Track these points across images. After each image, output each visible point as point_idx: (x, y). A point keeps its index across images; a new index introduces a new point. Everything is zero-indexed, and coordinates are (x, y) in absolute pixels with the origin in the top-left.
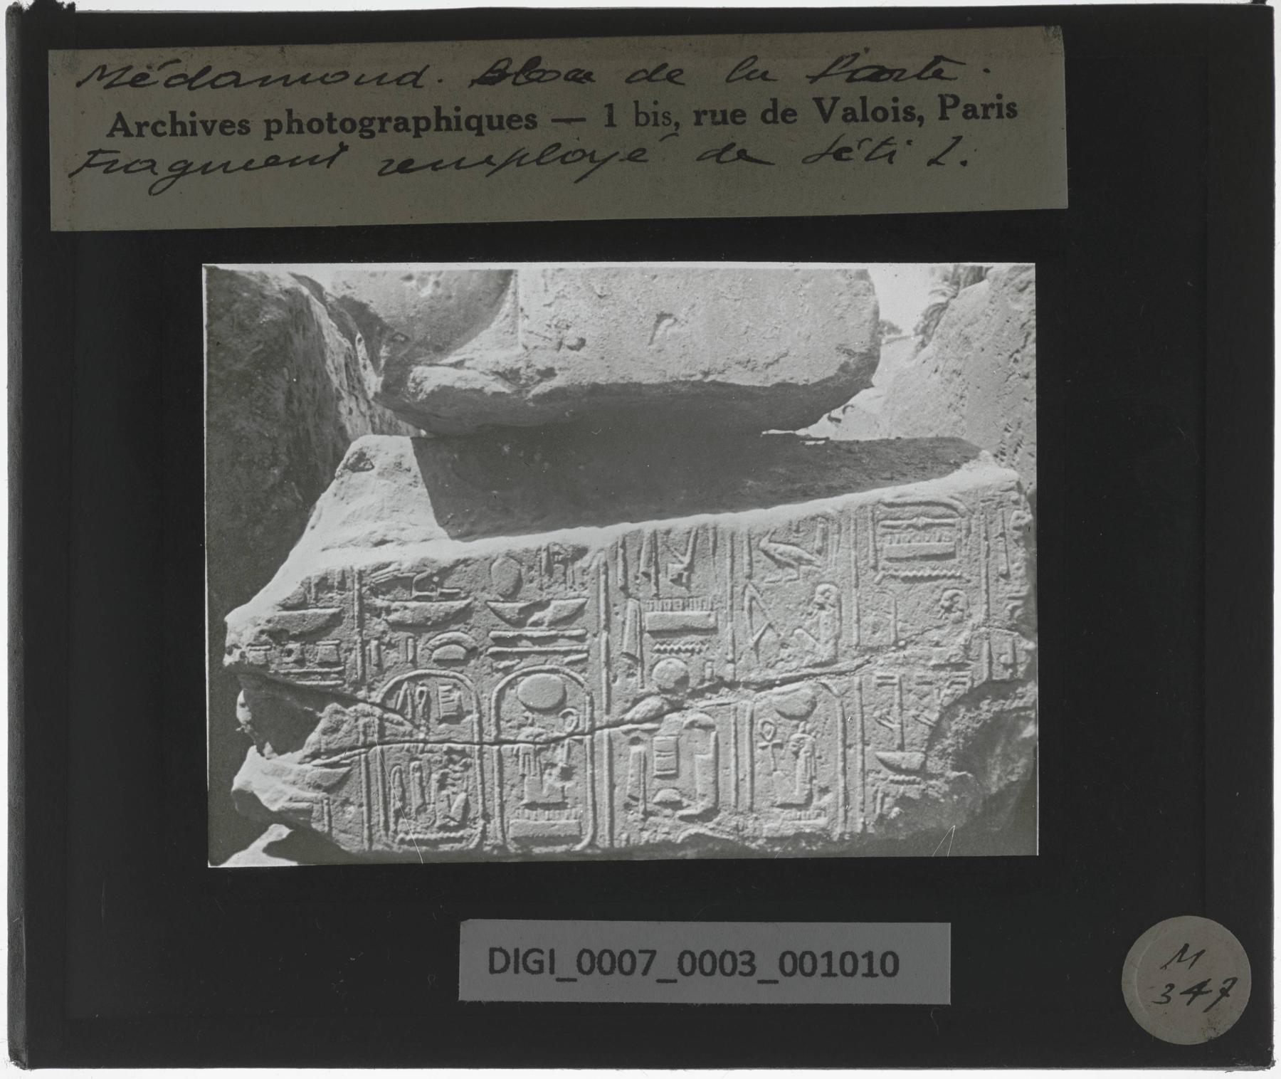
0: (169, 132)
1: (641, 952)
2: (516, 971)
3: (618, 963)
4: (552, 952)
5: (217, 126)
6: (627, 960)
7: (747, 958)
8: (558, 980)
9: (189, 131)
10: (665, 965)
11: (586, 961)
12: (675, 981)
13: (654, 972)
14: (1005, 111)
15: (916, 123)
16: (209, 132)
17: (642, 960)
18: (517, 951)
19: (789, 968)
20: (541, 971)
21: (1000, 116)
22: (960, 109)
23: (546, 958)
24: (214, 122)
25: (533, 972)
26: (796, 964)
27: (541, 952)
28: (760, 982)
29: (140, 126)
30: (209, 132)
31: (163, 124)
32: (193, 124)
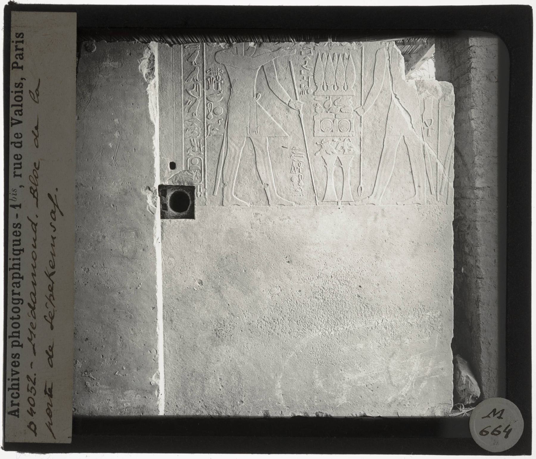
0: (17, 391)
5: (14, 369)
9: (16, 382)
14: (21, 39)
15: (23, 81)
16: (17, 373)
21: (22, 42)
22: (18, 61)
24: (12, 370)
29: (13, 405)
30: (17, 373)
31: (13, 394)
32: (12, 380)
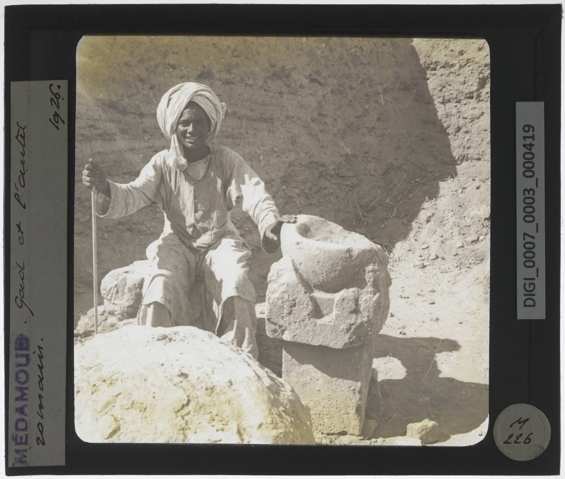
1: (524, 240)
2: (534, 295)
3: (530, 249)
4: (525, 279)
6: (528, 246)
7: (526, 192)
8: (537, 276)
10: (530, 228)
11: (528, 264)
12: (537, 224)
13: (532, 232)
17: (528, 239)
18: (525, 295)
19: (531, 174)
20: (533, 284)
23: (528, 282)
25: (534, 288)
26: (529, 171)
27: (525, 284)
28: (537, 187)
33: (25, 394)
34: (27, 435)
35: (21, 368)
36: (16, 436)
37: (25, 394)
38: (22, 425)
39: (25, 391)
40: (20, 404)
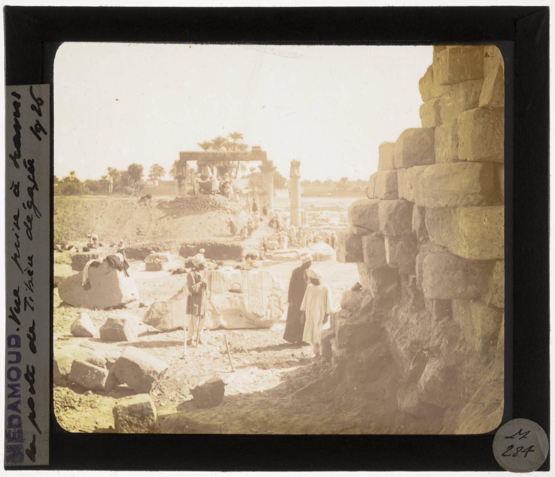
33: (19, 390)
34: (20, 432)
35: (12, 365)
36: (9, 431)
37: (19, 390)
38: (15, 421)
39: (17, 388)
40: (13, 400)
